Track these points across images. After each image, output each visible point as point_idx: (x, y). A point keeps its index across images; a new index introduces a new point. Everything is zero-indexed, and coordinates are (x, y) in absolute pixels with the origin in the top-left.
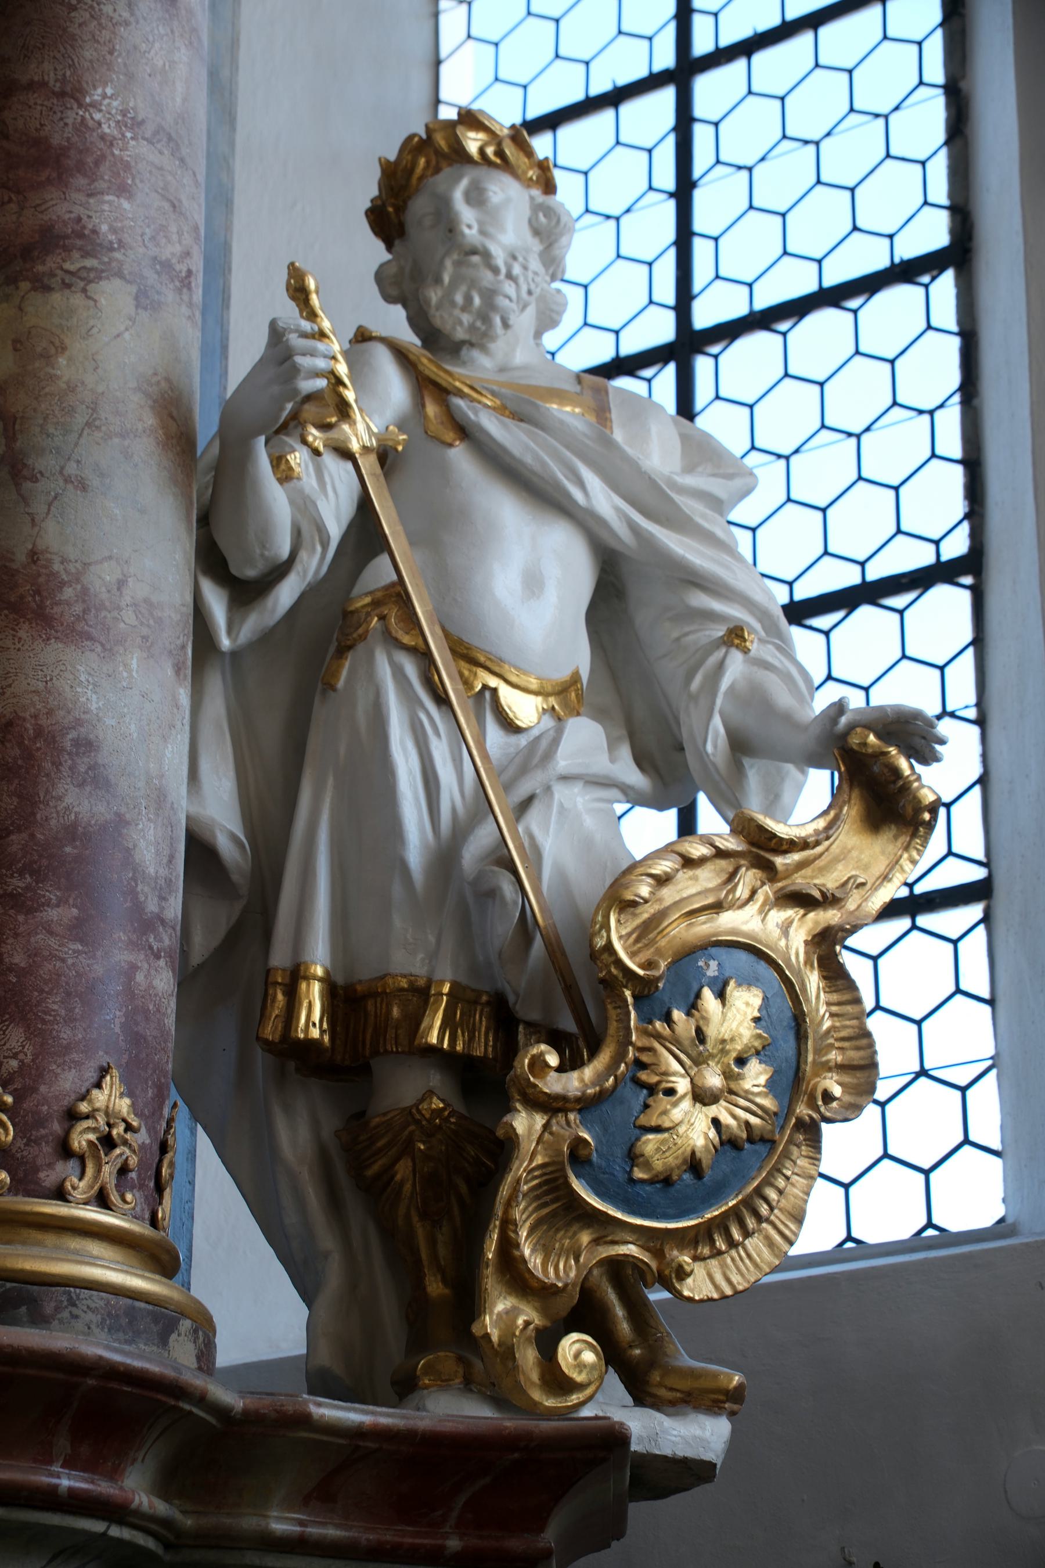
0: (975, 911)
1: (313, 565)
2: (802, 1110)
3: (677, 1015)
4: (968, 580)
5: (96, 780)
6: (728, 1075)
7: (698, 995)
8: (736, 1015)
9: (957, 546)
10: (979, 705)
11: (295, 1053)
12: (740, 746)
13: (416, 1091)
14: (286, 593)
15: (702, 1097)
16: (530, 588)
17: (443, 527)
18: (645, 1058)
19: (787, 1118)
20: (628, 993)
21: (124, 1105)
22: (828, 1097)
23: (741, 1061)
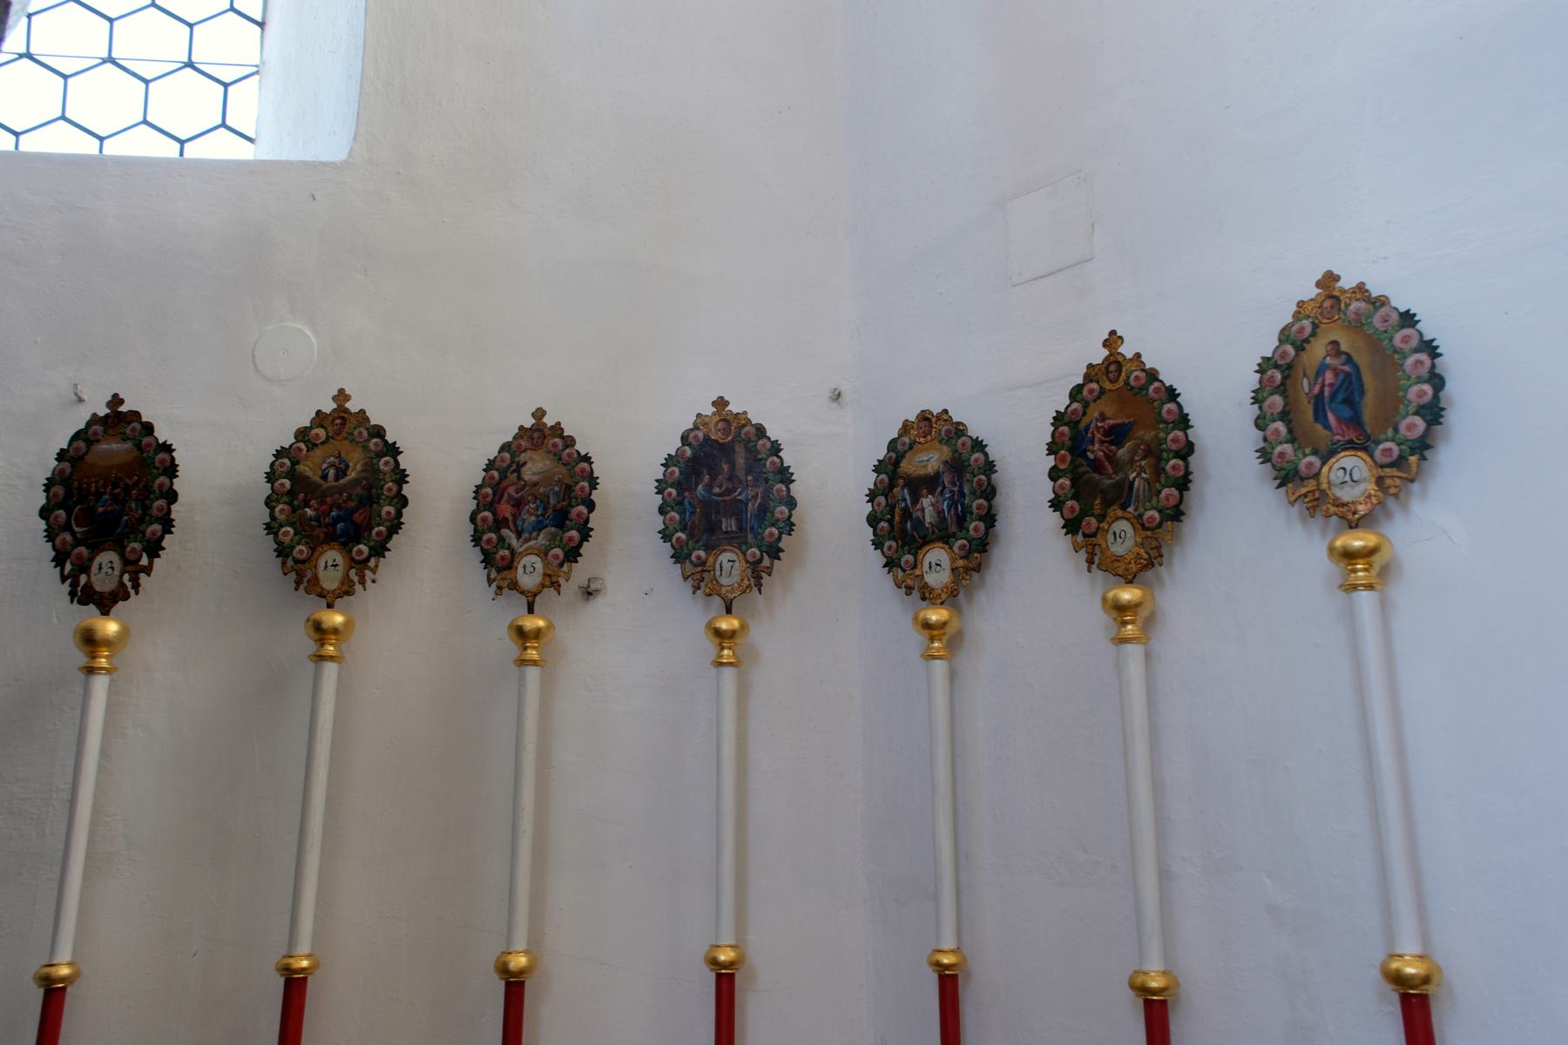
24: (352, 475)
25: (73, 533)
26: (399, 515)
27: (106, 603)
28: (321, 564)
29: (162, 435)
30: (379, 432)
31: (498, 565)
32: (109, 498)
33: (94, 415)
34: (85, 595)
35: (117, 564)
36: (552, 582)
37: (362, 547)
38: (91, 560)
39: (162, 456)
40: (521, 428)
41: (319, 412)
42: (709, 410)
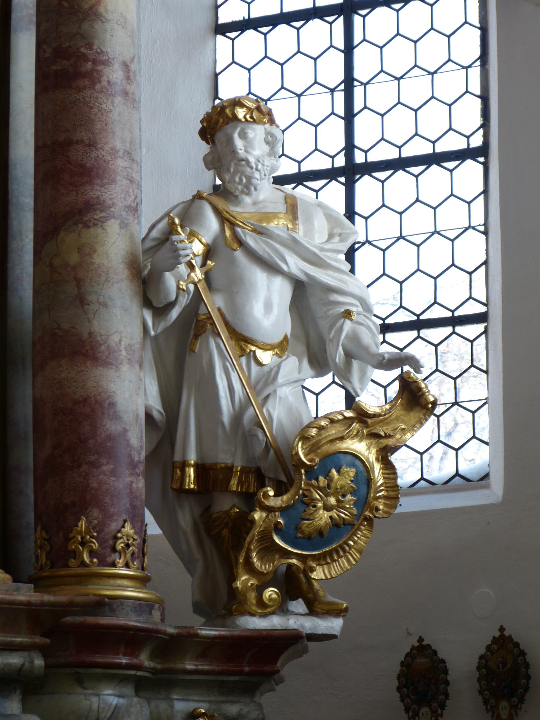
0: (480, 328)
1: (184, 301)
3: (321, 478)
4: (482, 159)
5: (116, 417)
6: (338, 501)
7: (330, 472)
8: (343, 478)
9: (477, 141)
10: (485, 224)
11: (182, 491)
12: (349, 356)
13: (226, 504)
14: (175, 313)
16: (268, 306)
17: (234, 288)
19: (360, 516)
20: (303, 471)
21: (132, 532)
23: (344, 496)
24: (509, 666)
25: (411, 699)
26: (528, 683)
28: (500, 708)
29: (441, 655)
30: (517, 645)
33: (413, 646)
35: (429, 713)
37: (515, 699)
38: (419, 711)
39: (441, 665)
41: (494, 637)
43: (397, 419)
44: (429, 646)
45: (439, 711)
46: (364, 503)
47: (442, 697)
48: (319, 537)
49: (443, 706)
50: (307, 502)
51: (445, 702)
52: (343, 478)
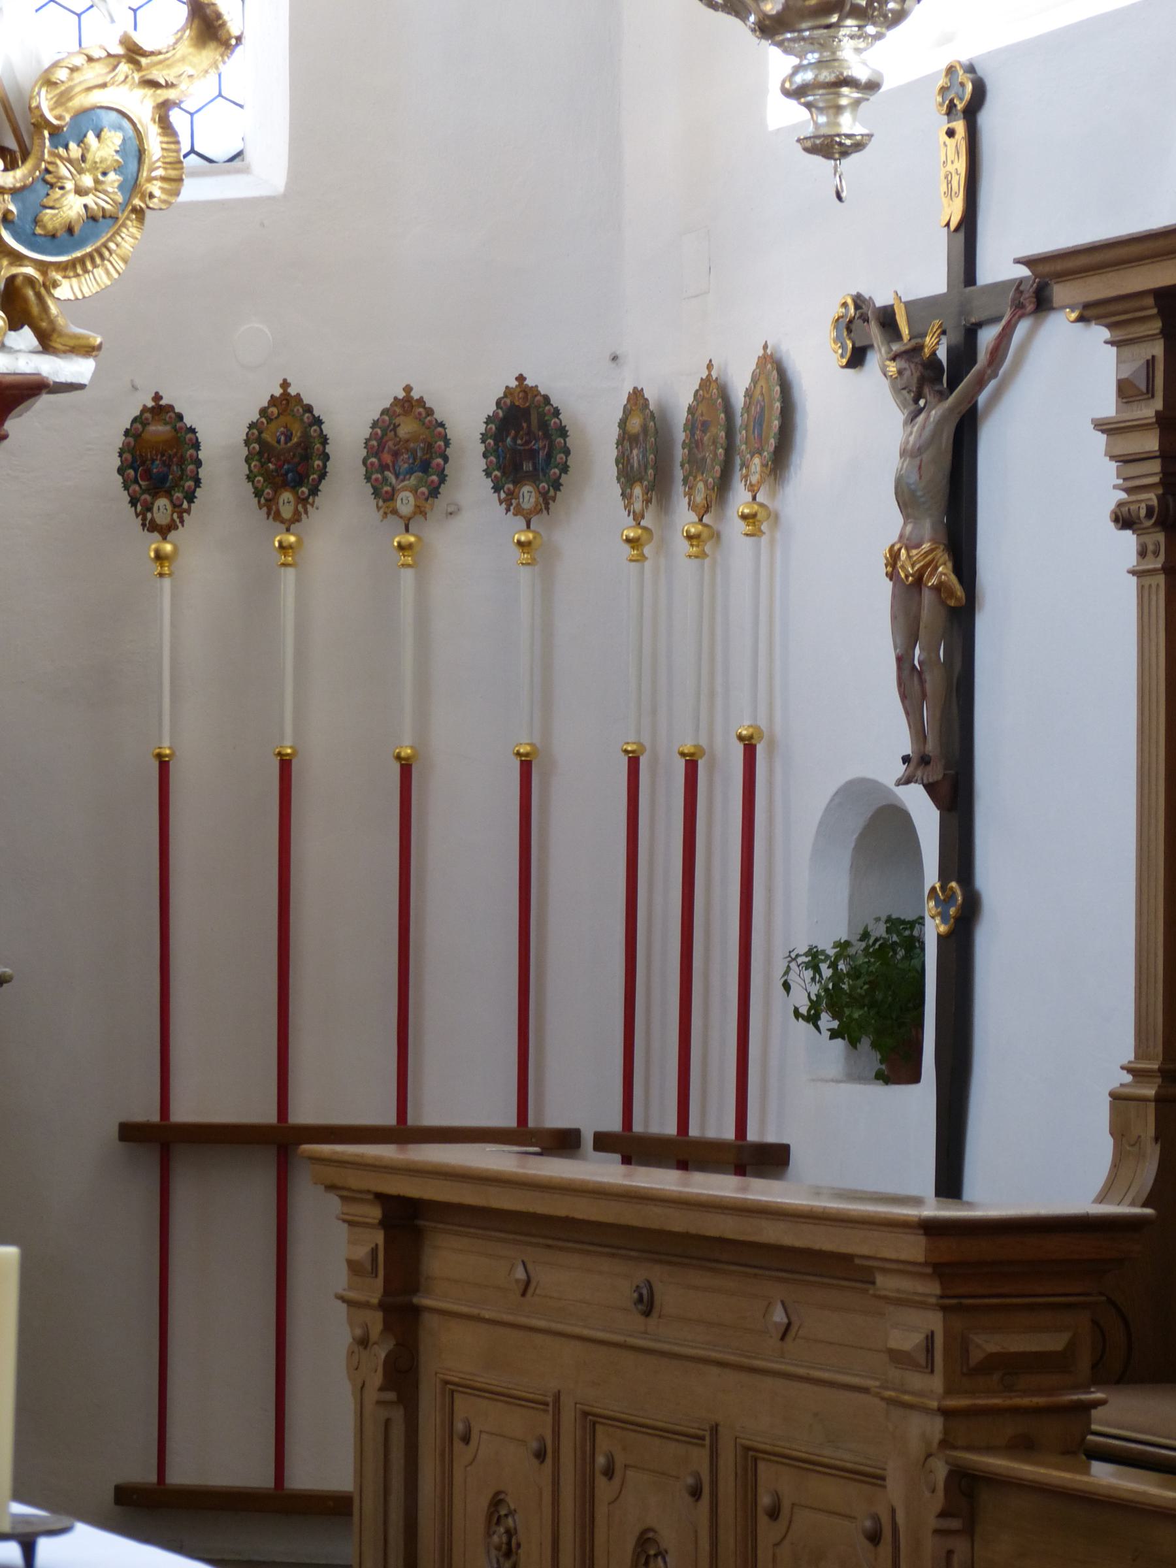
2: (137, 202)
3: (72, 145)
6: (97, 181)
7: (85, 136)
8: (106, 148)
15: (80, 191)
18: (51, 168)
19: (127, 205)
20: (46, 133)
22: (151, 196)
23: (104, 174)
24: (295, 440)
25: (140, 486)
26: (325, 466)
27: (164, 531)
28: (281, 501)
29: (189, 421)
30: (309, 409)
31: (384, 497)
32: (158, 462)
33: (145, 406)
34: (152, 527)
35: (169, 507)
36: (420, 511)
37: (304, 489)
38: (153, 504)
39: (190, 436)
40: (396, 398)
41: (272, 396)
42: (513, 384)
43: (183, 59)
44: (170, 408)
45: (185, 505)
46: (132, 186)
47: (191, 483)
48: (70, 234)
49: (191, 498)
50: (49, 181)
51: (194, 491)
52: (106, 148)
